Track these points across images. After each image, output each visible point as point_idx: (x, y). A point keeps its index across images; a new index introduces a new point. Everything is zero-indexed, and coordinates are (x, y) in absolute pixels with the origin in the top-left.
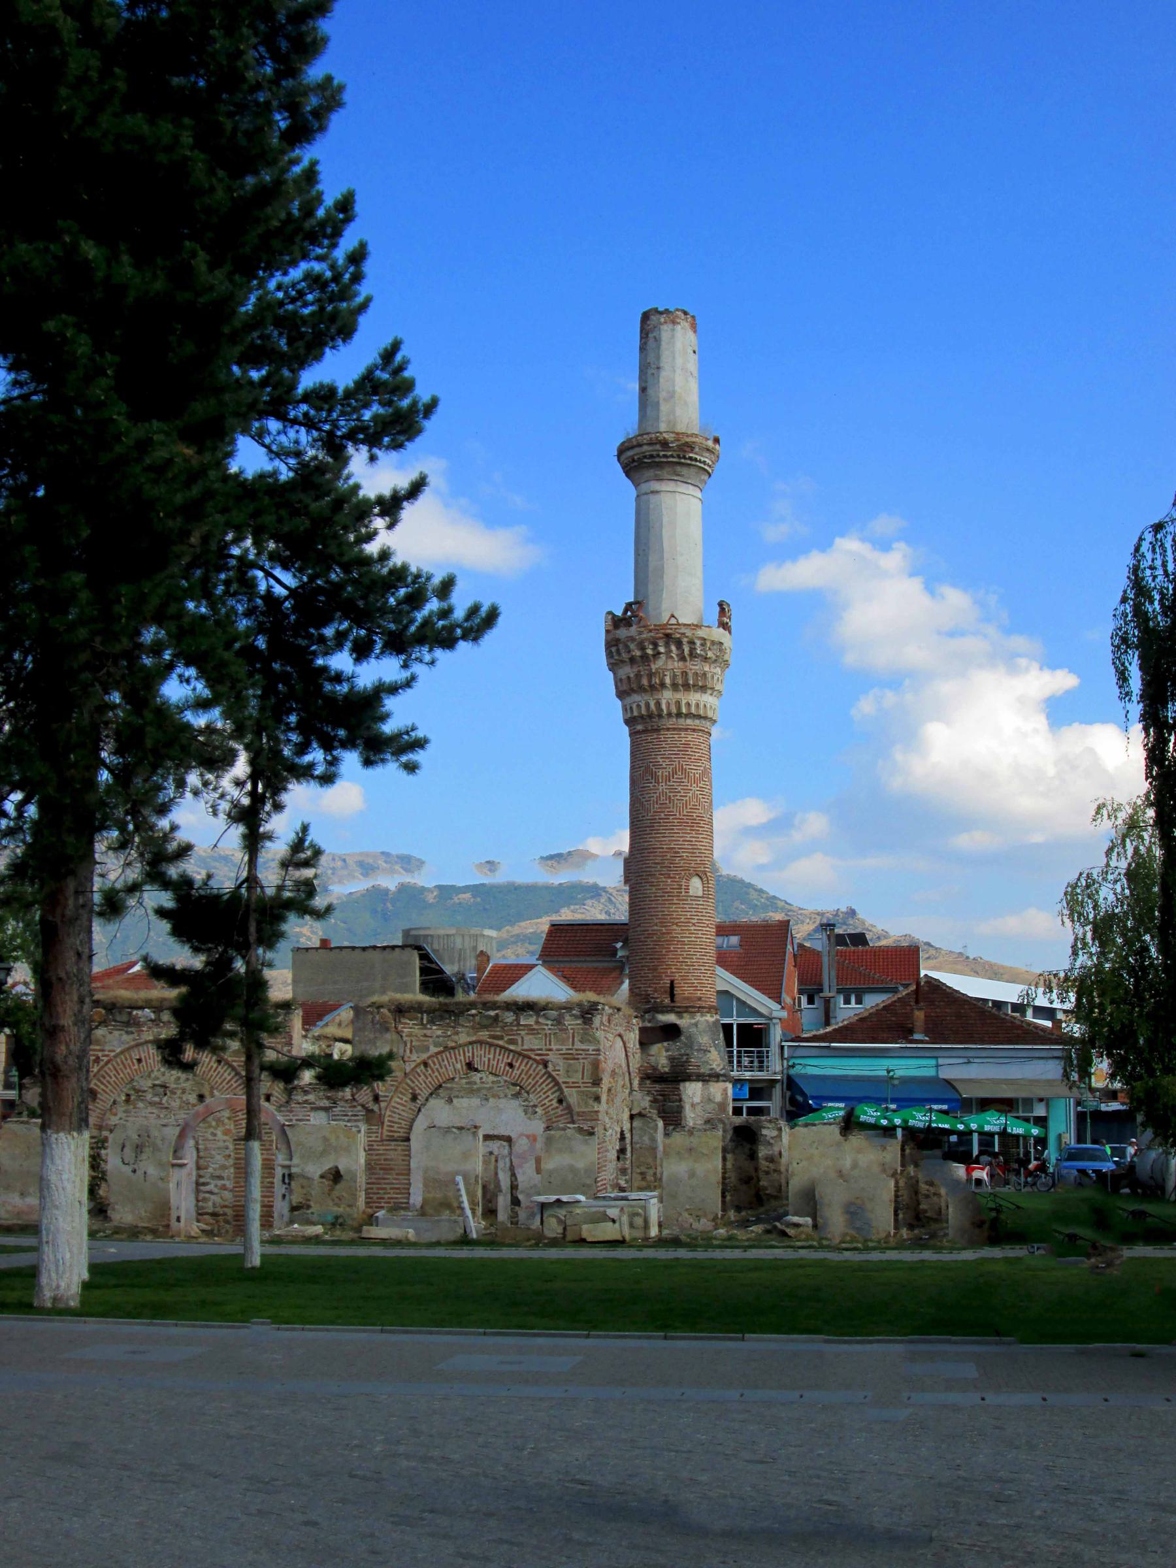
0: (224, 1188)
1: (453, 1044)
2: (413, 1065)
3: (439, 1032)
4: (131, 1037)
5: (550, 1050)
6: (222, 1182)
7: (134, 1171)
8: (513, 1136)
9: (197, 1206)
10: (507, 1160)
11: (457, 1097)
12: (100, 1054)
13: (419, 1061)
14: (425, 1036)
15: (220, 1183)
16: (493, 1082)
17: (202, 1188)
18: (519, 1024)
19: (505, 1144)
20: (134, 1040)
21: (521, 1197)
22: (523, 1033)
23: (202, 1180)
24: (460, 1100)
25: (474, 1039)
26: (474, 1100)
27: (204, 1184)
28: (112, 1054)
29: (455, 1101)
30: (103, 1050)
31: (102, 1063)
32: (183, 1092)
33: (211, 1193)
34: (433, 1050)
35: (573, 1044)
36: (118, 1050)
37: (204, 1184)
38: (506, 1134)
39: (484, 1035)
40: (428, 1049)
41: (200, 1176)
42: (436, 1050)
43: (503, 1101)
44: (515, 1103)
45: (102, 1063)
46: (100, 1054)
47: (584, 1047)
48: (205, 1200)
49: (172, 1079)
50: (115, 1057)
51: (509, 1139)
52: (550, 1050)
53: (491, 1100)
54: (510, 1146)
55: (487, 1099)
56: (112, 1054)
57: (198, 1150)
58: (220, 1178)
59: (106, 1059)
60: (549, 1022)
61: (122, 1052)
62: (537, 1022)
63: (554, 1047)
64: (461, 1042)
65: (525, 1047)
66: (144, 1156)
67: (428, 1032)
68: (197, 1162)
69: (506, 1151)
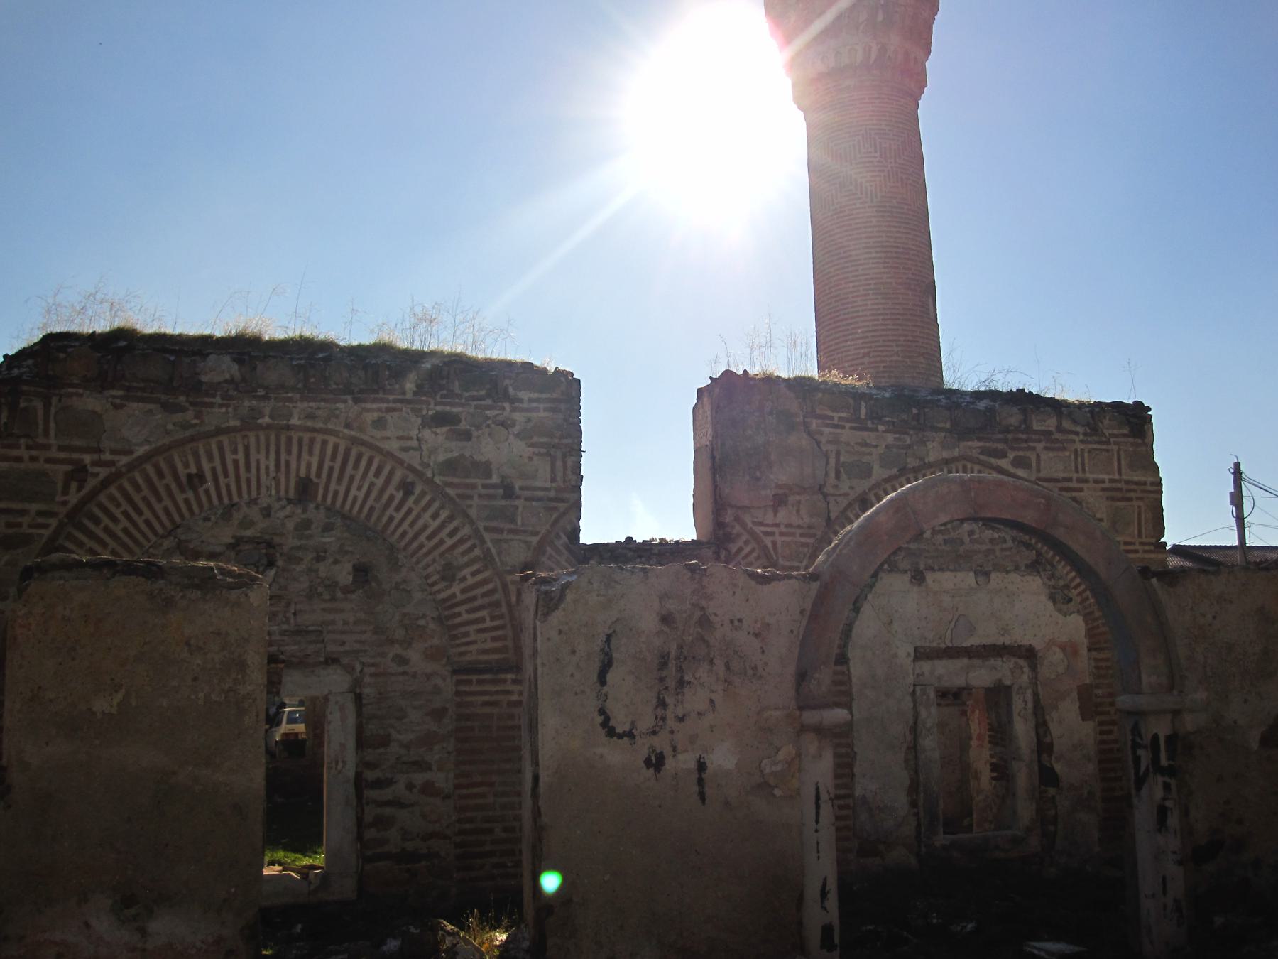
0: (428, 789)
1: (916, 463)
2: (844, 502)
3: (890, 438)
4: (178, 417)
5: (1086, 481)
6: (427, 776)
7: (656, 762)
8: (1038, 645)
9: (360, 837)
10: (1029, 692)
11: (932, 569)
12: (87, 458)
13: (853, 495)
14: (864, 444)
15: (419, 778)
16: (992, 541)
17: (370, 794)
18: (1029, 430)
19: (1022, 662)
20: (185, 426)
21: (1058, 768)
22: (1040, 446)
23: (370, 775)
24: (938, 575)
25: (956, 453)
26: (960, 575)
27: (378, 784)
28: (123, 460)
29: (930, 577)
30: (99, 450)
31: (92, 483)
32: (319, 559)
33: (397, 803)
34: (878, 473)
35: (1120, 473)
36: (141, 451)
37: (378, 784)
38: (1025, 642)
39: (972, 446)
40: (868, 473)
41: (364, 764)
42: (886, 474)
43: (1014, 577)
44: (1035, 583)
45: (92, 483)
46: (87, 458)
47: (1136, 479)
48: (381, 822)
49: (290, 525)
50: (131, 467)
51: (1029, 654)
52: (1086, 481)
53: (993, 576)
54: (1034, 668)
55: (987, 574)
56: (123, 460)
57: (358, 698)
58: (421, 766)
59: (103, 472)
60: (1079, 429)
61: (147, 458)
62: (1060, 429)
63: (1088, 475)
64: (931, 458)
65: (1043, 474)
66: (694, 700)
67: (869, 436)
68: (360, 730)
69: (1025, 678)
